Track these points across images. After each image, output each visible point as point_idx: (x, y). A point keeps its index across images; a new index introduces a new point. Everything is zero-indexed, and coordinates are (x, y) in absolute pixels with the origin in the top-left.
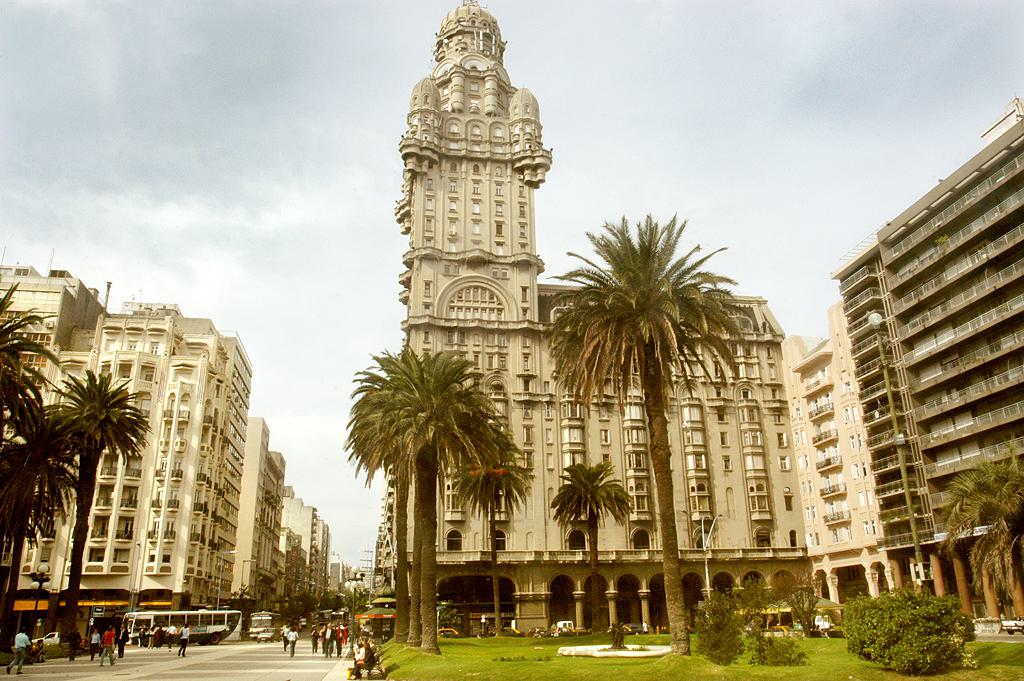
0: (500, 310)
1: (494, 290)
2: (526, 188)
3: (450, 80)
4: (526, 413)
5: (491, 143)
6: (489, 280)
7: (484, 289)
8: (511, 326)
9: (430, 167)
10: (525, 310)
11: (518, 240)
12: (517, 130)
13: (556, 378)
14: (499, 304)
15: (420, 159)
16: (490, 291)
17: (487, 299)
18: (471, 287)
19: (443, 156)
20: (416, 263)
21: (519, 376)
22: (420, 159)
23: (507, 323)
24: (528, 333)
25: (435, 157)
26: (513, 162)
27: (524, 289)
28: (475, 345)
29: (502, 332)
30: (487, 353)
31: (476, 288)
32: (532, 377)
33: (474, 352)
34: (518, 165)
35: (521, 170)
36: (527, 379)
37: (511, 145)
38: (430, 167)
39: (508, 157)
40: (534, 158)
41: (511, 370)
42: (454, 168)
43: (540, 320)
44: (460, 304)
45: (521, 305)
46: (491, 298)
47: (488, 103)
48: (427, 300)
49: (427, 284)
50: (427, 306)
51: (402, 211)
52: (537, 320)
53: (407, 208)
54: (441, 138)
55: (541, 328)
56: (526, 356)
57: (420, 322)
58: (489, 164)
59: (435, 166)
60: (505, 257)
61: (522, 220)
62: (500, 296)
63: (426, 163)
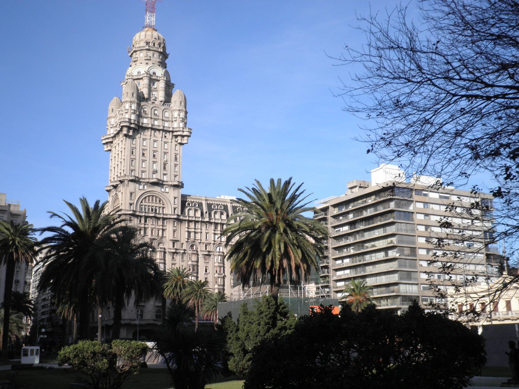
0: (163, 208)
1: (161, 198)
2: (178, 145)
3: (142, 79)
4: (173, 258)
5: (163, 120)
6: (159, 193)
7: (156, 197)
8: (168, 217)
10: (175, 209)
11: (173, 173)
12: (176, 114)
13: (187, 242)
14: (163, 205)
16: (159, 198)
17: (158, 202)
18: (150, 195)
20: (126, 182)
21: (171, 240)
23: (166, 215)
24: (178, 220)
25: (137, 128)
26: (173, 132)
27: (175, 198)
28: (152, 225)
29: (164, 219)
30: (157, 229)
32: (178, 241)
33: (151, 228)
34: (175, 134)
36: (174, 242)
37: (172, 122)
39: (171, 129)
40: (183, 132)
41: (167, 238)
43: (182, 213)
44: (145, 204)
45: (173, 206)
46: (160, 201)
47: (160, 95)
48: (132, 202)
49: (131, 194)
50: (131, 204)
51: (107, 141)
52: (180, 214)
53: (110, 140)
55: (181, 218)
56: (174, 231)
57: (128, 213)
58: (161, 132)
59: (136, 132)
60: (167, 182)
61: (176, 163)
62: (164, 201)
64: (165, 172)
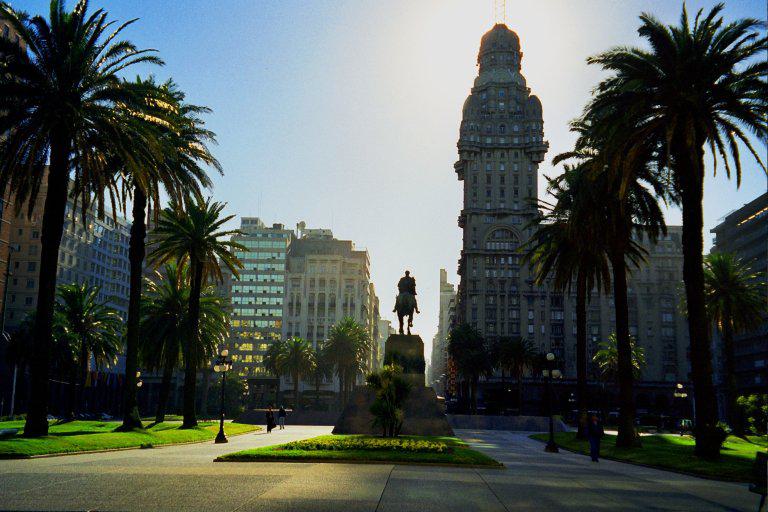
9: (475, 155)
15: (469, 152)
19: (481, 149)
21: (526, 281)
22: (469, 152)
25: (478, 150)
26: (525, 148)
31: (503, 230)
35: (529, 154)
38: (475, 155)
42: (489, 156)
49: (475, 229)
54: (481, 136)
63: (473, 154)
64: (516, 199)
